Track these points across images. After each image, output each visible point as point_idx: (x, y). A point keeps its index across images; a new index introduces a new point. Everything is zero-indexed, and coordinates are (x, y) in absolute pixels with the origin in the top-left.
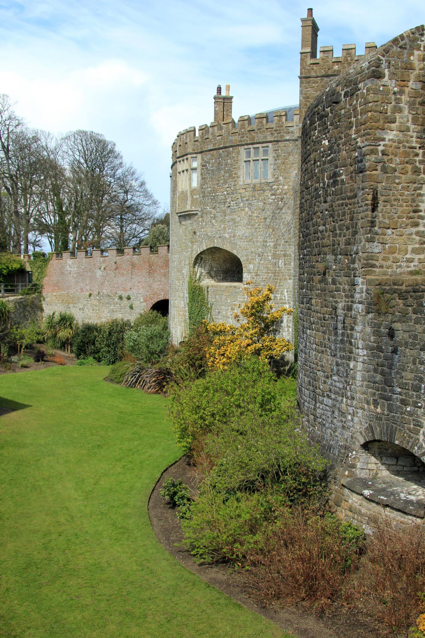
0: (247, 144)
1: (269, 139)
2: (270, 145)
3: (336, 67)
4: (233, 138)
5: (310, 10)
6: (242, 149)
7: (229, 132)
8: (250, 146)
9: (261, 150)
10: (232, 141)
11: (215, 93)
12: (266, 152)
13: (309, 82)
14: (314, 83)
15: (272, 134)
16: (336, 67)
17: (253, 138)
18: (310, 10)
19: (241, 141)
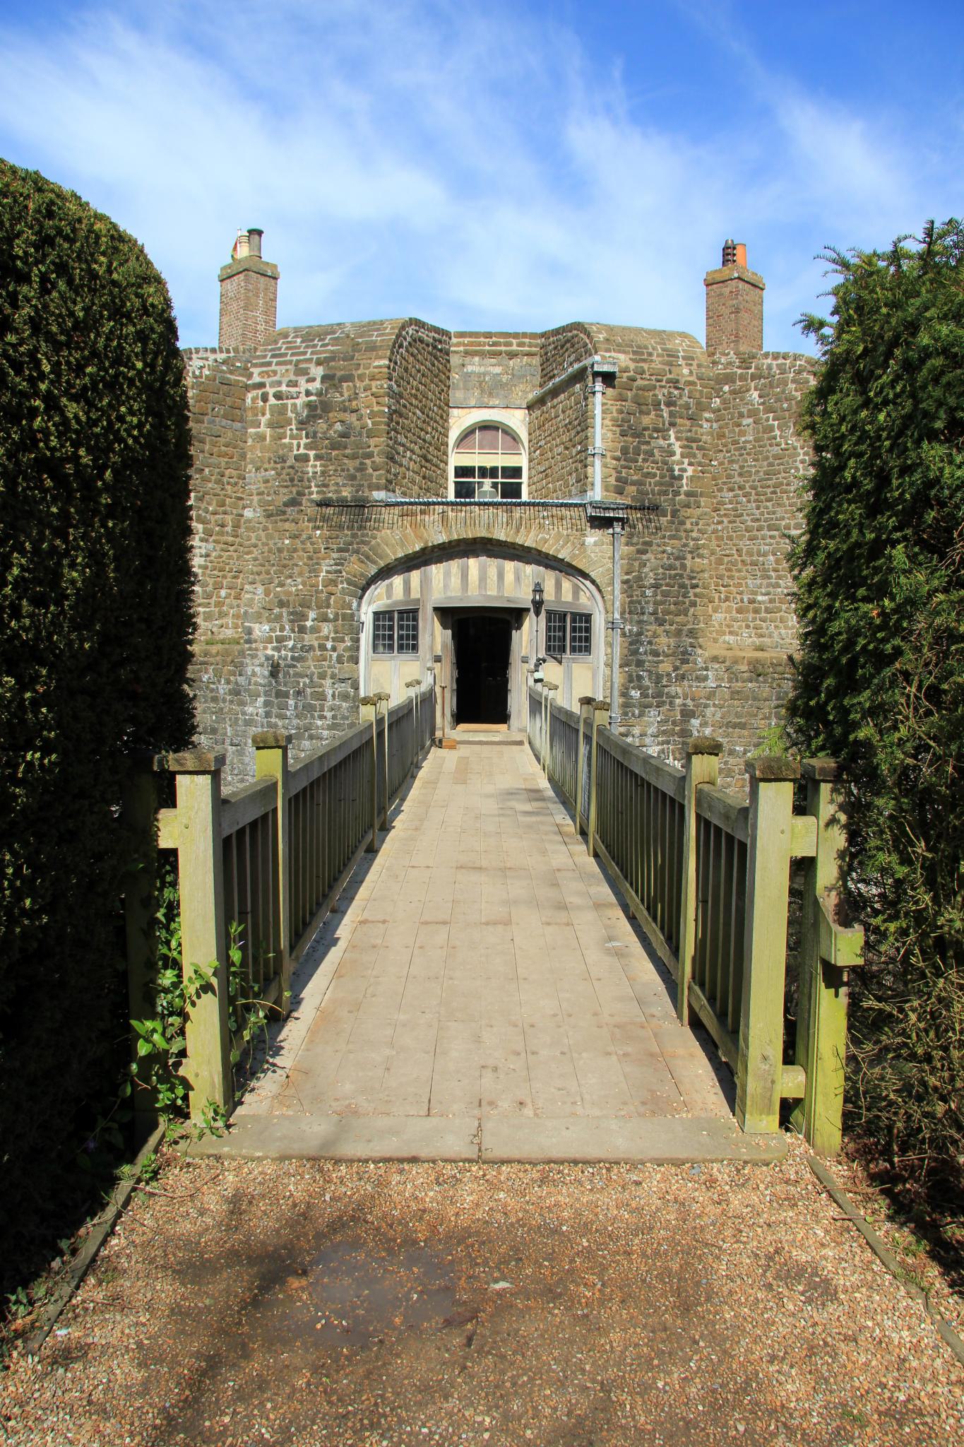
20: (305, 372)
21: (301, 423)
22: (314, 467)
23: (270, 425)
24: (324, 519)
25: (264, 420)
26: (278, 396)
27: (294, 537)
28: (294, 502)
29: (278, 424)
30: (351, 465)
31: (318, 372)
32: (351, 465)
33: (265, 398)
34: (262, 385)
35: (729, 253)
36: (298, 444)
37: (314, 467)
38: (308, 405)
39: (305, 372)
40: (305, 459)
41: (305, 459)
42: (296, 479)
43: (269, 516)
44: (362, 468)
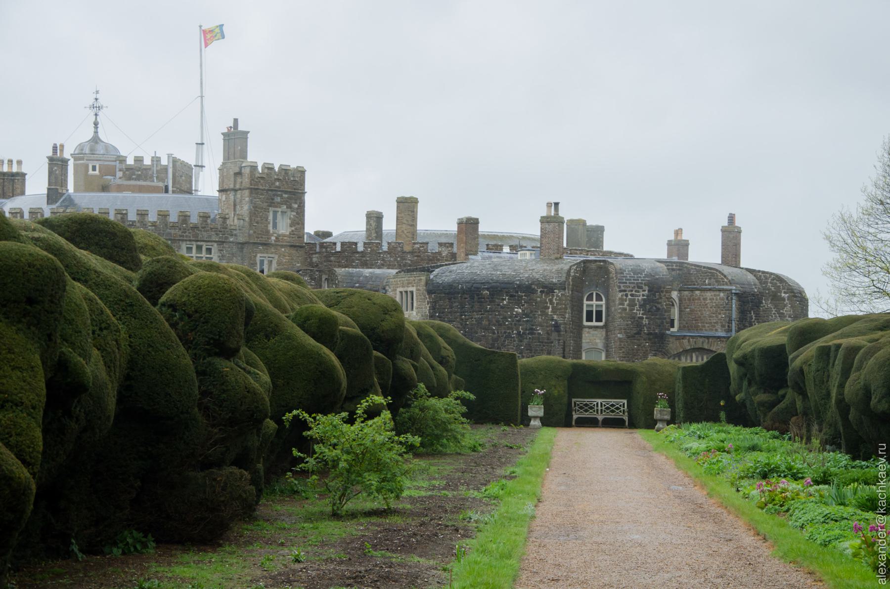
0: (190, 241)
1: (214, 238)
2: (215, 245)
3: (277, 184)
4: (173, 231)
5: (236, 121)
6: (184, 246)
7: (166, 225)
8: (194, 243)
9: (204, 249)
10: (170, 234)
11: (50, 154)
12: (209, 251)
13: (257, 194)
14: (262, 194)
15: (217, 234)
16: (277, 184)
17: (196, 236)
18: (236, 121)
19: (183, 236)
20: (641, 288)
21: (641, 306)
22: (645, 321)
23: (628, 305)
24: (650, 339)
25: (626, 303)
26: (632, 295)
27: (638, 345)
28: (638, 333)
29: (632, 304)
30: (659, 321)
31: (647, 288)
32: (659, 321)
33: (626, 295)
34: (625, 291)
35: (731, 218)
36: (640, 314)
37: (645, 321)
38: (644, 300)
39: (641, 288)
40: (642, 318)
41: (642, 318)
42: (638, 323)
43: (628, 337)
44: (662, 323)
